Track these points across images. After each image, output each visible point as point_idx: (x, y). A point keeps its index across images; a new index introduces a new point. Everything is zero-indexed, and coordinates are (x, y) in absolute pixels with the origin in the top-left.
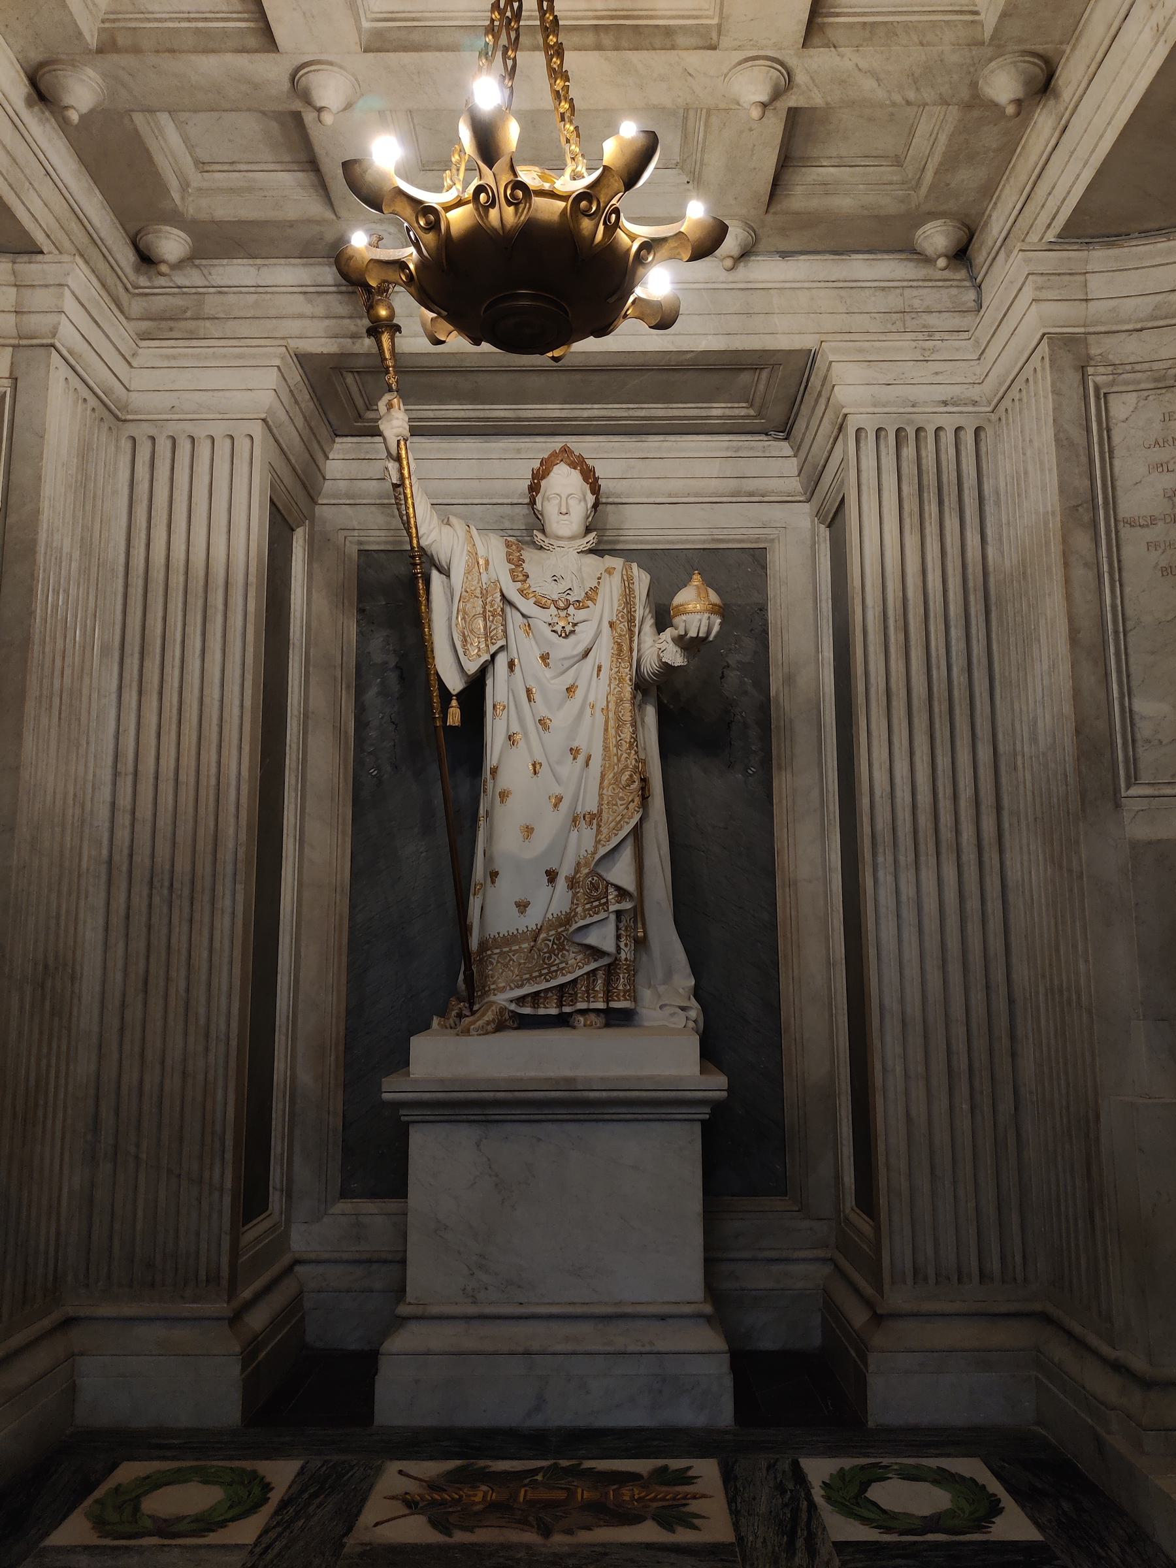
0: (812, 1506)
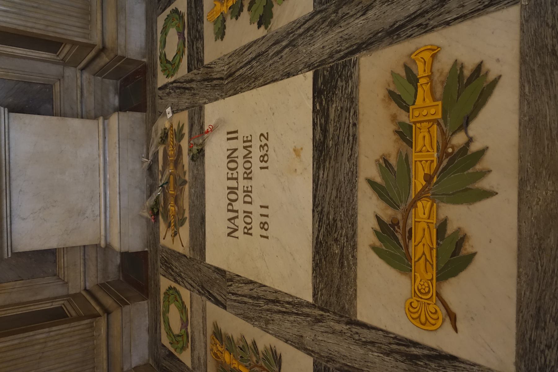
0: (175, 82)
